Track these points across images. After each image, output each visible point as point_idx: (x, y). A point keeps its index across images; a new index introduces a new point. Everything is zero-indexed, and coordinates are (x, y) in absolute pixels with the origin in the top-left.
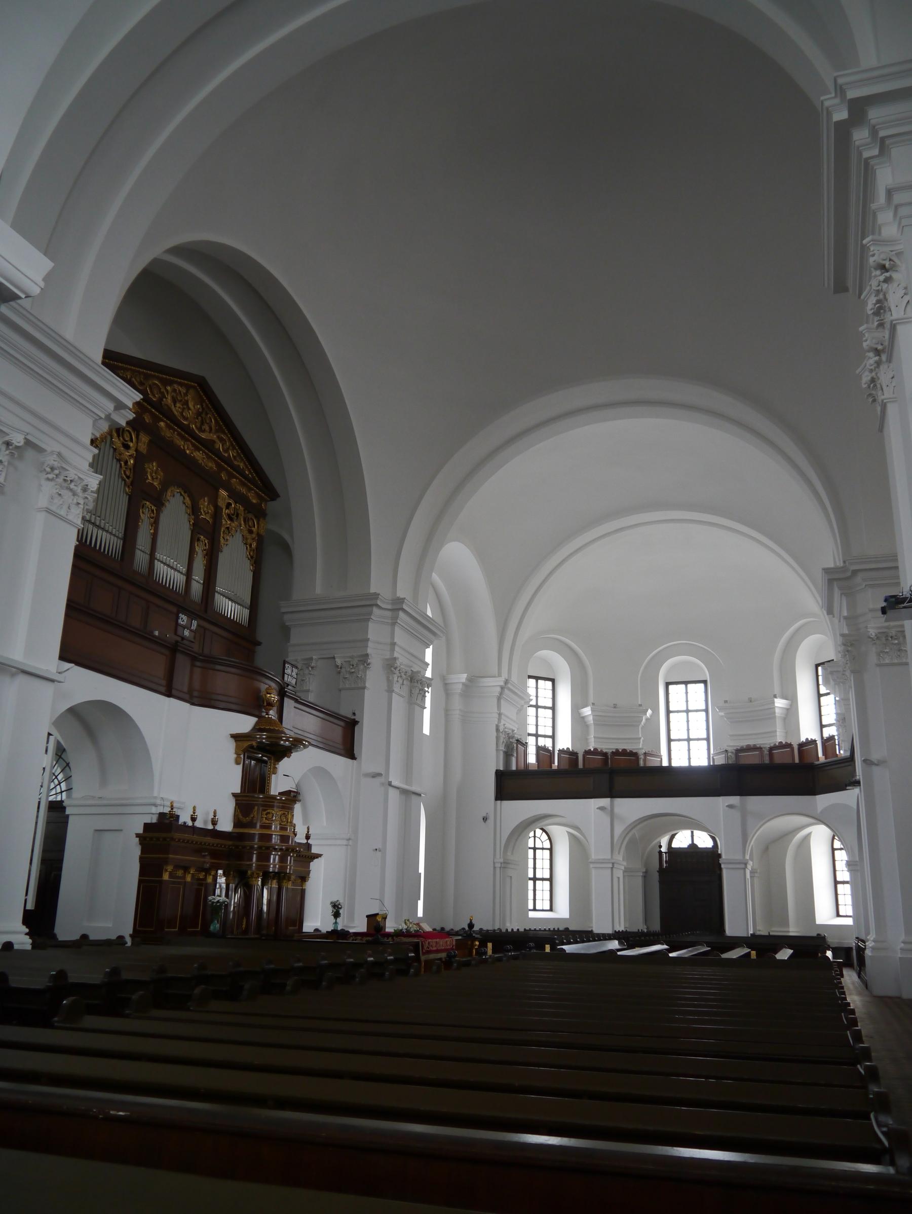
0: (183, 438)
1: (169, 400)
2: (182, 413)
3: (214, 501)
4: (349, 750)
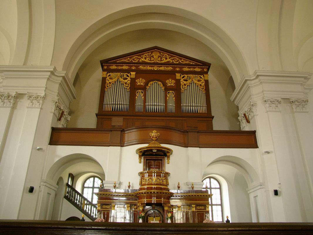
0: (152, 66)
2: (151, 60)
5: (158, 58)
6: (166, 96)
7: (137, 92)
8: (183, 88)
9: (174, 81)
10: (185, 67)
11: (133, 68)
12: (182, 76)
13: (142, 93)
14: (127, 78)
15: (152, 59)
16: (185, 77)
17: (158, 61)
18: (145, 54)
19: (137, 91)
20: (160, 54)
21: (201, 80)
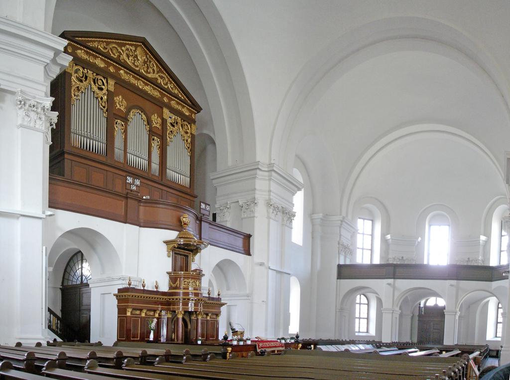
0: (136, 79)
1: (124, 56)
2: (134, 64)
3: (161, 116)
4: (247, 252)
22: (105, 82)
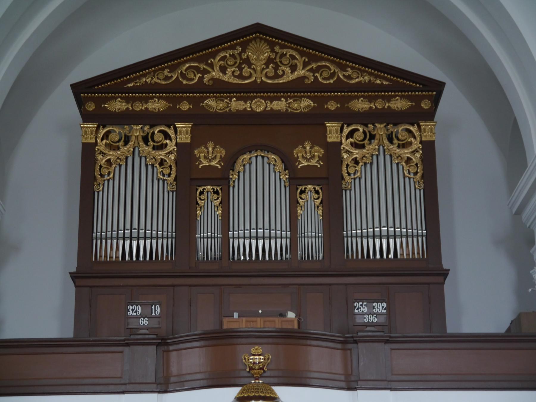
2: (241, 77)
5: (267, 64)
6: (294, 204)
7: (201, 193)
8: (349, 174)
9: (319, 151)
10: (358, 98)
11: (185, 107)
12: (346, 130)
13: (216, 196)
14: (166, 145)
15: (246, 70)
16: (356, 135)
17: (267, 77)
18: (222, 54)
19: (201, 189)
20: (273, 51)
21: (410, 143)
22: (171, 132)
